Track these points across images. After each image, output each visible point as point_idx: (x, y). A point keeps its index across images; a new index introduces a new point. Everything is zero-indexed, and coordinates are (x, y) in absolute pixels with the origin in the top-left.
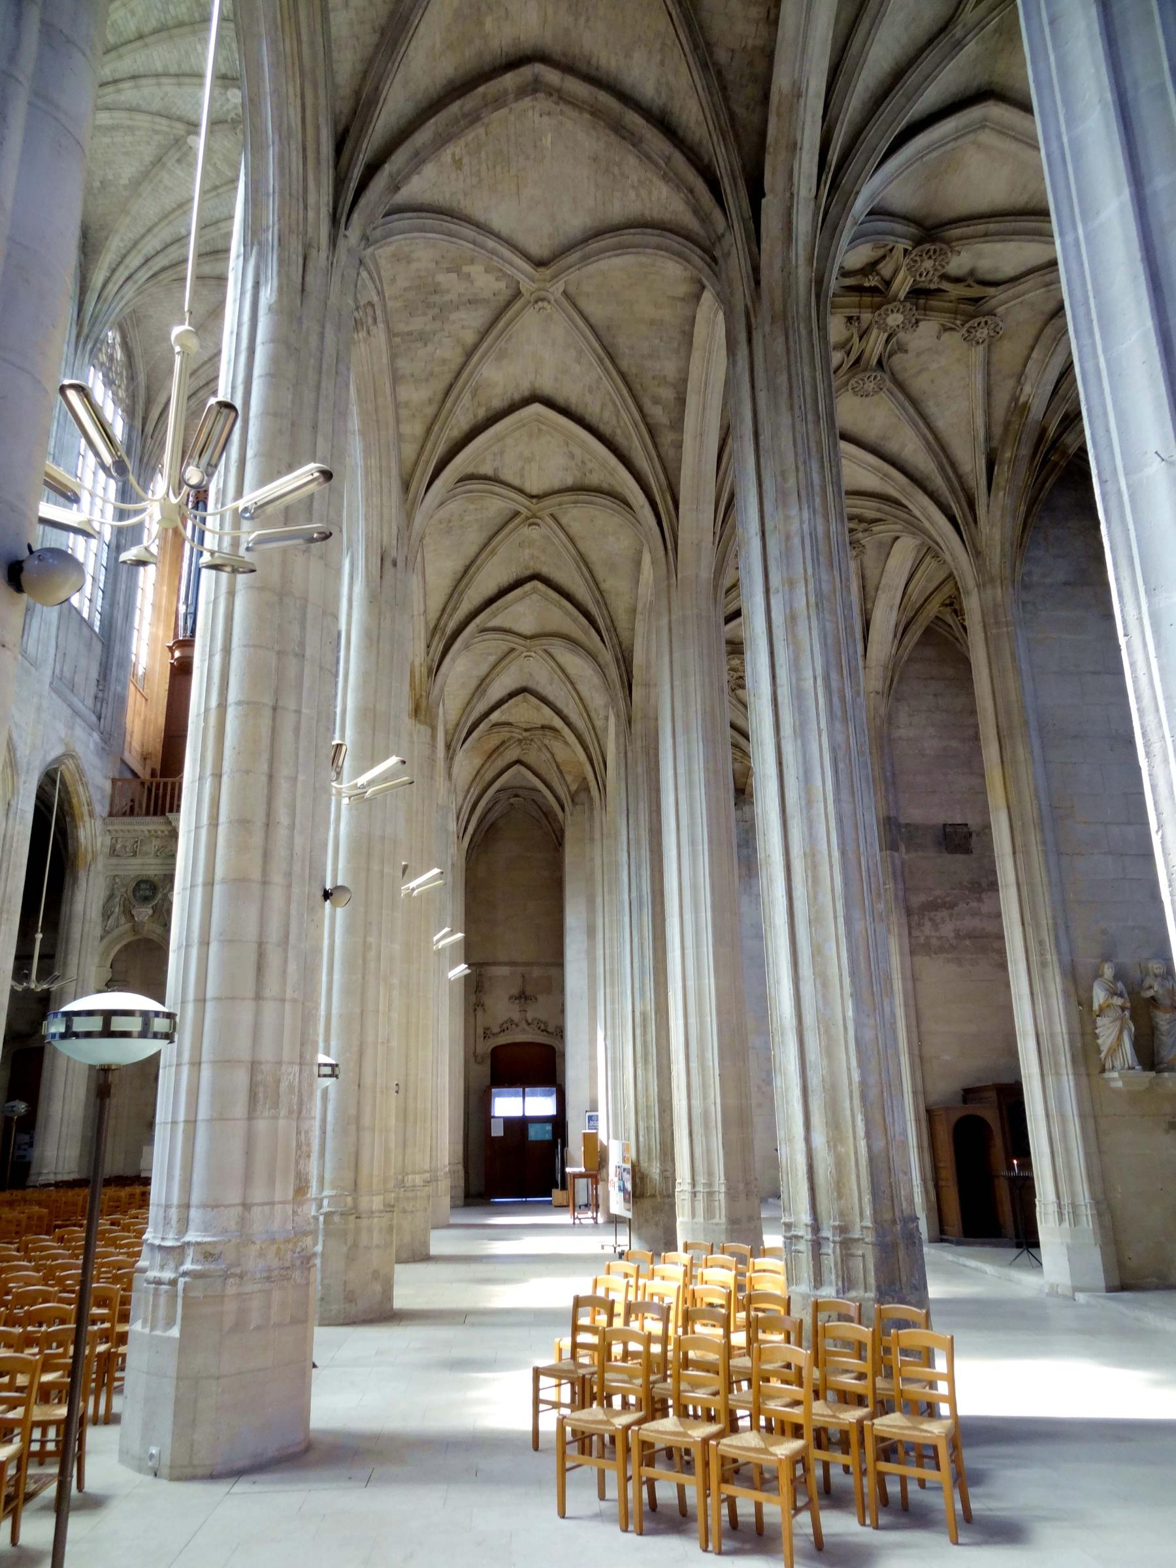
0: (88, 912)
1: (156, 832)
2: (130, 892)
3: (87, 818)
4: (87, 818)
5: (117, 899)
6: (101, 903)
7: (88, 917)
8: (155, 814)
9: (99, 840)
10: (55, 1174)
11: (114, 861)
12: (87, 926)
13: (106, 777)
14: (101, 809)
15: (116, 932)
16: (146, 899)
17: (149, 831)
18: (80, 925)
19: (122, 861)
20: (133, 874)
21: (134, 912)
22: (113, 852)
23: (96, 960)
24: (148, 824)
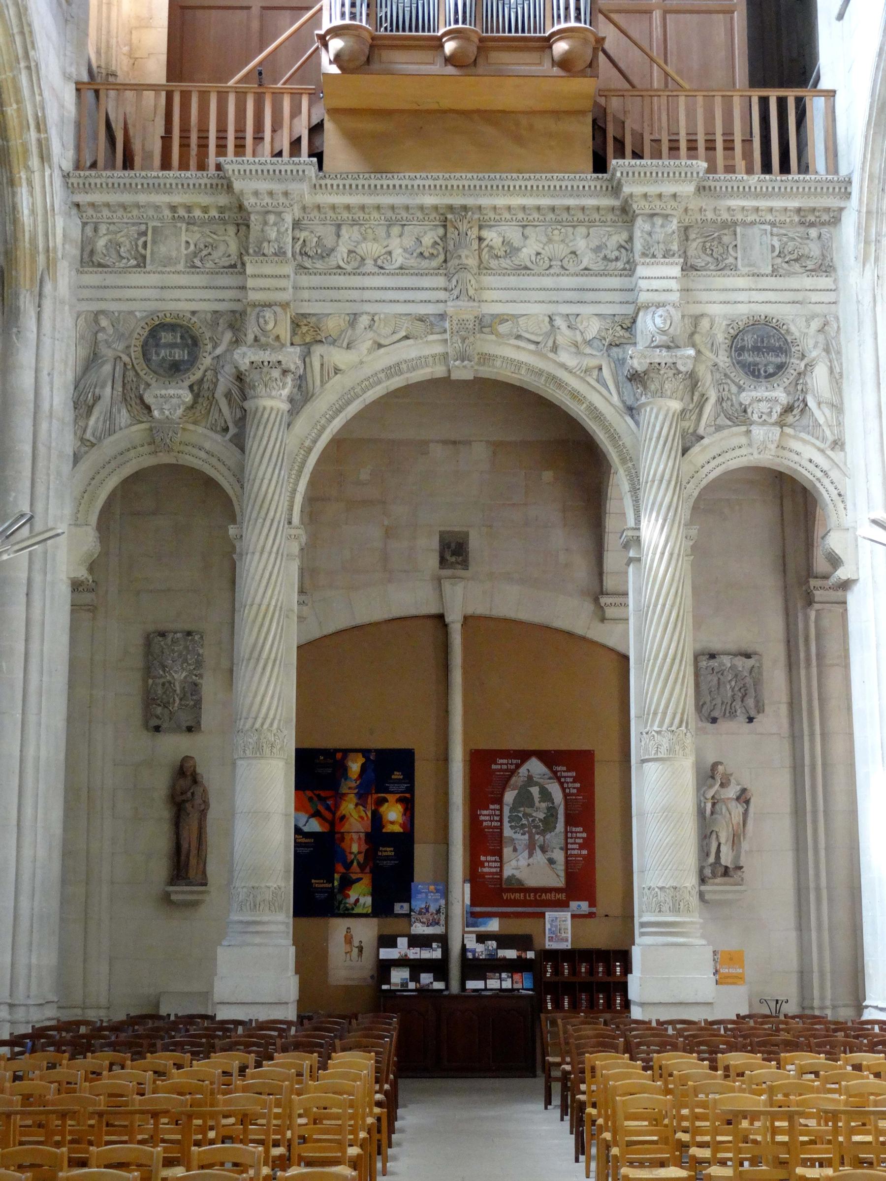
0: (45, 391)
1: (189, 209)
2: (136, 352)
3: (35, 162)
4: (35, 162)
5: (107, 368)
6: (70, 376)
7: (46, 406)
8: (184, 165)
9: (60, 223)
10: (11, 1006)
11: (93, 278)
12: (44, 426)
13: (67, 77)
14: (62, 152)
15: (110, 446)
16: (175, 369)
17: (173, 208)
18: (28, 423)
19: (111, 279)
20: (141, 309)
21: (149, 399)
22: (89, 259)
23: (68, 511)
24: (168, 189)
